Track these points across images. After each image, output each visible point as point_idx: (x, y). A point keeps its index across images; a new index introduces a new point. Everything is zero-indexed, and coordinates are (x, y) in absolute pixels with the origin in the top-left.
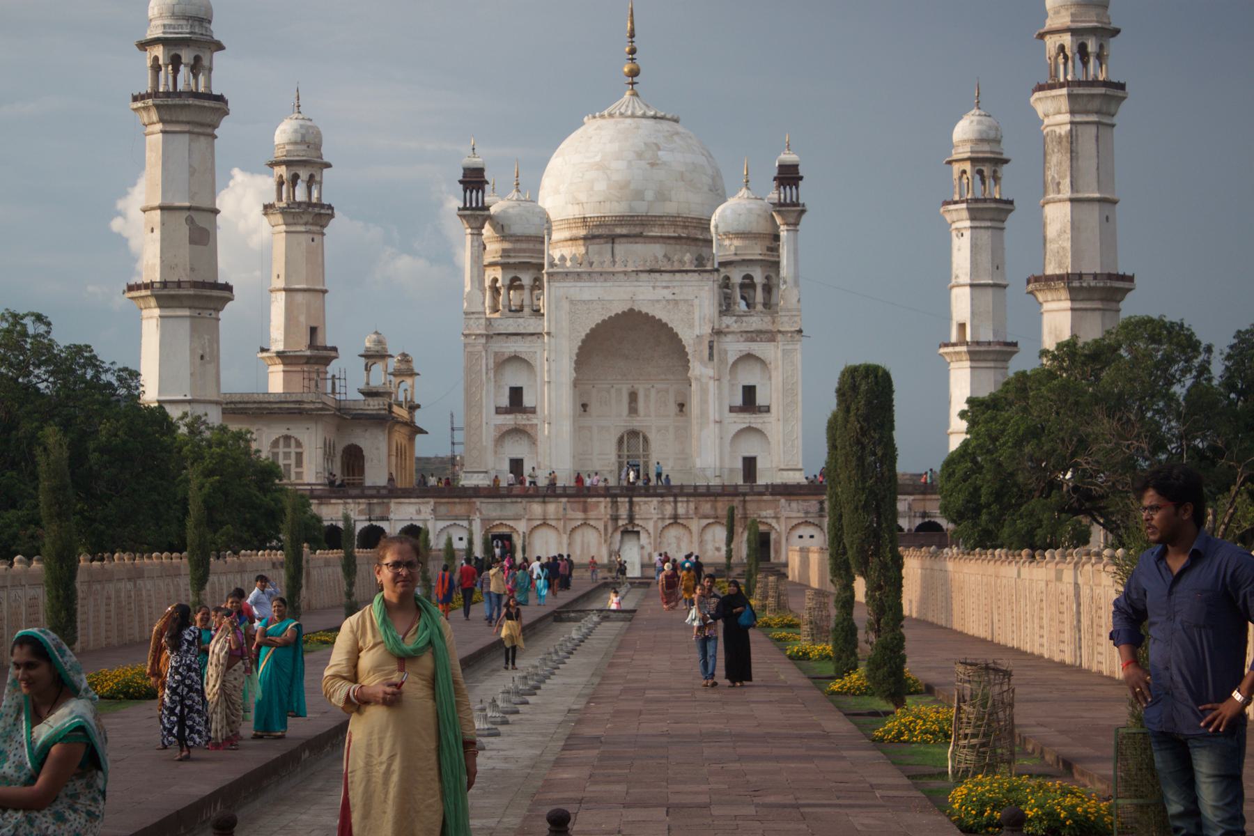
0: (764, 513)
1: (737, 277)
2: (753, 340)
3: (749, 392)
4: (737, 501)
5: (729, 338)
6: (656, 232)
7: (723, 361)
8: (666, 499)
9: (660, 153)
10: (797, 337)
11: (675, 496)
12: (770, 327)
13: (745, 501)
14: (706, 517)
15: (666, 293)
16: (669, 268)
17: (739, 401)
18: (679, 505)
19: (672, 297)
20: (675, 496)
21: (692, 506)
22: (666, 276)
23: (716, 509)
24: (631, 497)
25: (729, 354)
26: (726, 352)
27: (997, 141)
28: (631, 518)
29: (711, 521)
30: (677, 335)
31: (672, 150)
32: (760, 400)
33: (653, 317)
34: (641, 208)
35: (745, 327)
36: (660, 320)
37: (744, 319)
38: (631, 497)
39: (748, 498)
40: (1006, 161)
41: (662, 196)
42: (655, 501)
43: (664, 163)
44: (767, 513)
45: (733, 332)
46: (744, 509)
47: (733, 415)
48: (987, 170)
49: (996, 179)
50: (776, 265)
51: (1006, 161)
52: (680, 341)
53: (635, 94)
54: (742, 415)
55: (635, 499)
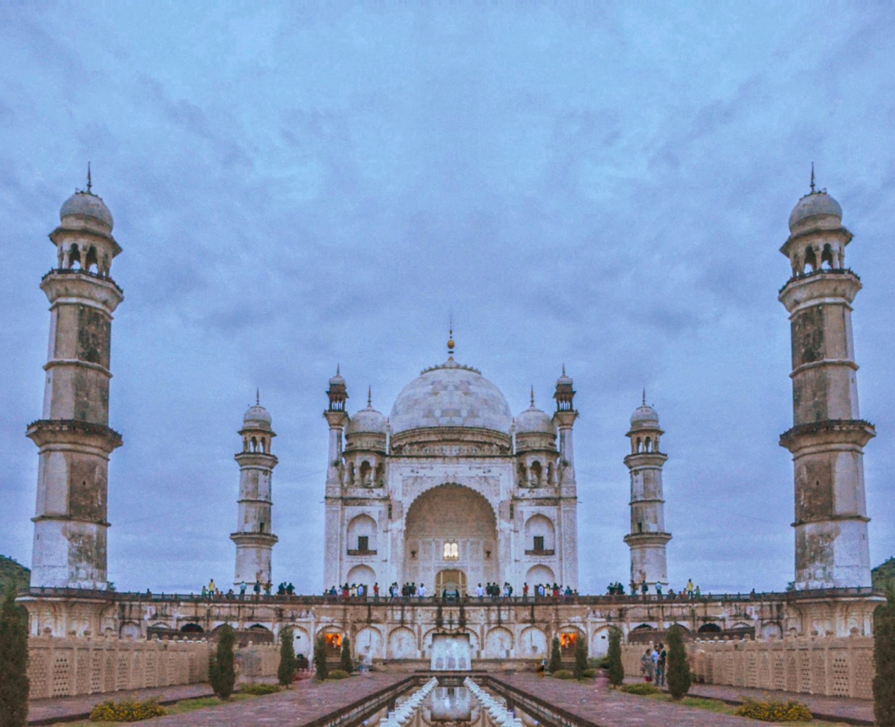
0: (573, 619)
1: (529, 462)
2: (542, 505)
3: (539, 541)
4: (551, 607)
5: (525, 503)
6: (469, 438)
7: (522, 520)
8: (492, 608)
9: (471, 387)
10: (572, 501)
11: (499, 605)
12: (554, 495)
13: (557, 610)
14: (525, 622)
15: (480, 473)
16: (480, 453)
17: (531, 547)
18: (502, 612)
19: (483, 475)
20: (499, 605)
21: (513, 613)
22: (478, 460)
23: (532, 615)
24: (462, 606)
25: (525, 514)
26: (522, 512)
27: (656, 421)
28: (462, 623)
29: (529, 625)
30: (487, 500)
31: (478, 386)
32: (547, 546)
33: (470, 489)
34: (458, 422)
35: (534, 495)
36: (475, 491)
37: (535, 490)
38: (462, 606)
39: (560, 607)
40: (661, 433)
41: (473, 414)
42: (482, 610)
43: (474, 393)
44: (578, 618)
45: (527, 499)
46: (557, 615)
47: (529, 556)
48: (653, 436)
49: (656, 443)
50: (555, 454)
51: (661, 433)
52: (490, 505)
53: (451, 358)
54: (534, 557)
55: (466, 608)
